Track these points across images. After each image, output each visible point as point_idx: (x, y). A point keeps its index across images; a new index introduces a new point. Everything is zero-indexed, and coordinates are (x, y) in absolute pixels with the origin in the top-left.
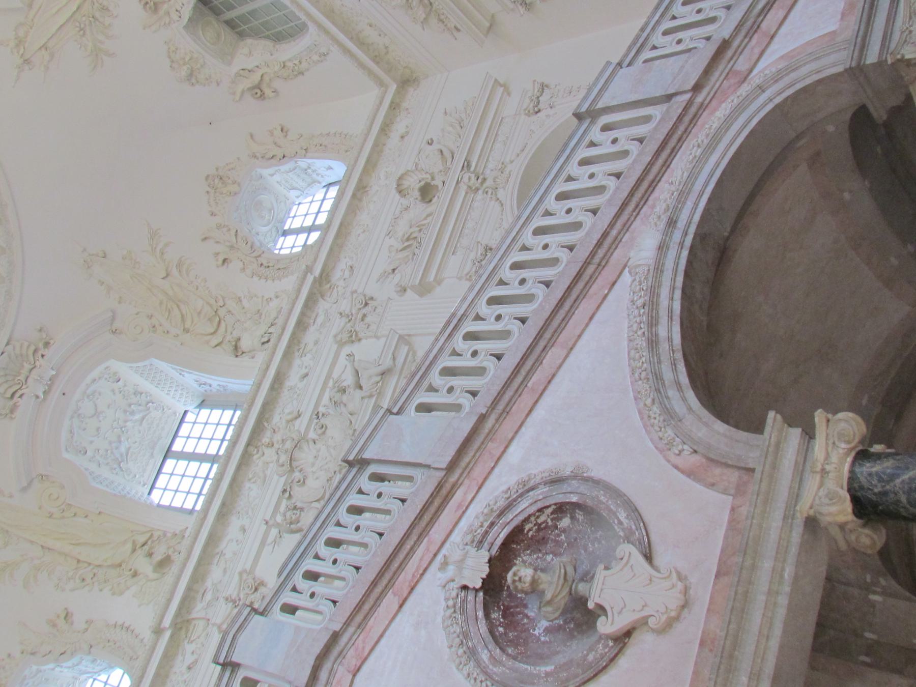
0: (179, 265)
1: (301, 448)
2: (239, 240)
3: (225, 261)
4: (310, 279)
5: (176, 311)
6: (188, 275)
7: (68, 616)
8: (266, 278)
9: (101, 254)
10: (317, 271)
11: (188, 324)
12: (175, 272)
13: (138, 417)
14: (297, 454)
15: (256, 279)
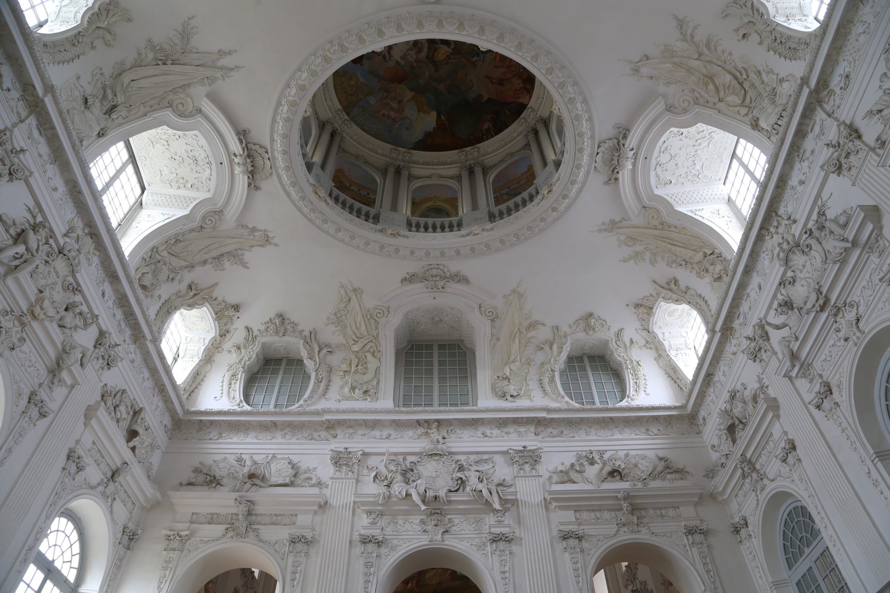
0: (708, 45)
1: (794, 252)
2: (755, 12)
3: (744, 36)
4: (806, 91)
5: (711, 87)
6: (716, 50)
7: (676, 282)
8: (780, 54)
9: (644, 59)
10: (813, 83)
11: (722, 94)
12: (706, 50)
13: (705, 144)
14: (791, 256)
15: (772, 53)
